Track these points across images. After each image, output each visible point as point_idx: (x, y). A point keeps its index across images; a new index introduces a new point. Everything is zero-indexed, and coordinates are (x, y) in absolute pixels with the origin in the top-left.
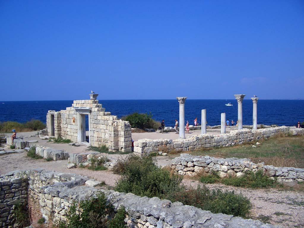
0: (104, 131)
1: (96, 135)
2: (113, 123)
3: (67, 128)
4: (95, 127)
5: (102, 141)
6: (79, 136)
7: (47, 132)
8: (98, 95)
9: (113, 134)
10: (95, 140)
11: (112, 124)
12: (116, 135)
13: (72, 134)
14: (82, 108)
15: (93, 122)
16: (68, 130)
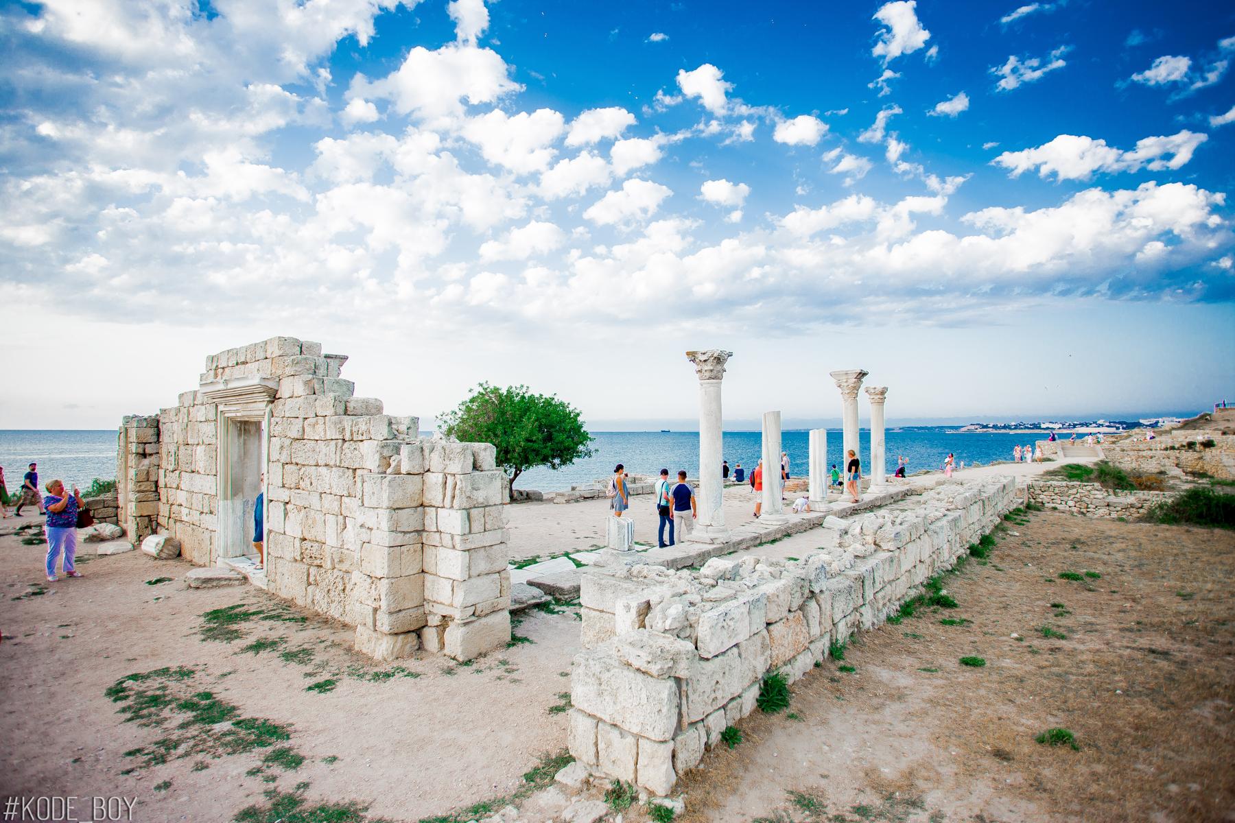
0: (336, 504)
1: (294, 528)
2: (386, 453)
3: (178, 488)
4: (291, 481)
5: (328, 565)
6: (219, 528)
7: (117, 507)
8: (346, 358)
9: (385, 525)
10: (289, 555)
11: (386, 461)
12: (414, 537)
13: (195, 517)
14: (231, 386)
15: (284, 458)
16: (181, 497)
